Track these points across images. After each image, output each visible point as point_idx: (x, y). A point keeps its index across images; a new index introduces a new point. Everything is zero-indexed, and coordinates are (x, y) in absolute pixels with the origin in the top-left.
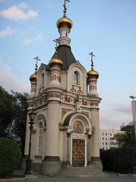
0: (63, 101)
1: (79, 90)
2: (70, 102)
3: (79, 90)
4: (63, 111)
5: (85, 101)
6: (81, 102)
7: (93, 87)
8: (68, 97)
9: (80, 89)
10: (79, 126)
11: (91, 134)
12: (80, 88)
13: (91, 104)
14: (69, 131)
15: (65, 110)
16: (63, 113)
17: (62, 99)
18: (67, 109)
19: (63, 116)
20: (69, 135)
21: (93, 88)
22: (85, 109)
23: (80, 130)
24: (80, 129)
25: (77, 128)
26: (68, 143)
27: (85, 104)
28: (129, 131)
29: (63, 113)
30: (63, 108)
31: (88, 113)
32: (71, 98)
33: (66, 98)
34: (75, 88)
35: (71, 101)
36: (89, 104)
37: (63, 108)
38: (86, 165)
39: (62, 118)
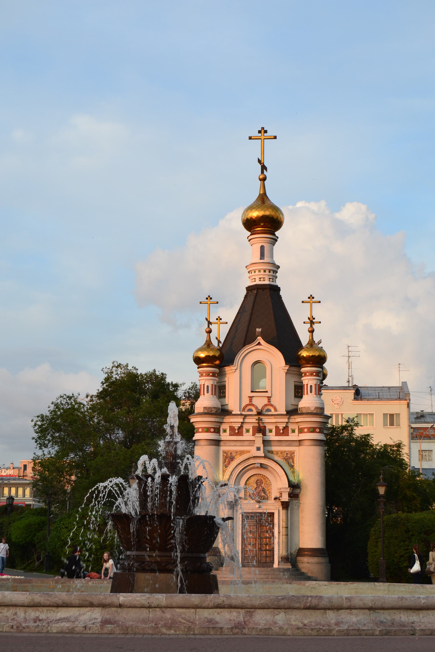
0: (225, 436)
1: (266, 402)
2: (242, 435)
3: (266, 402)
4: (225, 458)
5: (281, 426)
6: (274, 431)
7: (307, 389)
9: (269, 401)
10: (263, 485)
11: (287, 500)
12: (269, 398)
13: (301, 431)
15: (231, 453)
16: (227, 460)
17: (225, 431)
19: (226, 467)
21: (316, 387)
22: (284, 443)
23: (264, 493)
24: (264, 491)
27: (285, 431)
29: (227, 460)
30: (224, 452)
33: (232, 429)
34: (255, 401)
35: (248, 431)
36: (297, 431)
38: (276, 565)
39: (224, 472)
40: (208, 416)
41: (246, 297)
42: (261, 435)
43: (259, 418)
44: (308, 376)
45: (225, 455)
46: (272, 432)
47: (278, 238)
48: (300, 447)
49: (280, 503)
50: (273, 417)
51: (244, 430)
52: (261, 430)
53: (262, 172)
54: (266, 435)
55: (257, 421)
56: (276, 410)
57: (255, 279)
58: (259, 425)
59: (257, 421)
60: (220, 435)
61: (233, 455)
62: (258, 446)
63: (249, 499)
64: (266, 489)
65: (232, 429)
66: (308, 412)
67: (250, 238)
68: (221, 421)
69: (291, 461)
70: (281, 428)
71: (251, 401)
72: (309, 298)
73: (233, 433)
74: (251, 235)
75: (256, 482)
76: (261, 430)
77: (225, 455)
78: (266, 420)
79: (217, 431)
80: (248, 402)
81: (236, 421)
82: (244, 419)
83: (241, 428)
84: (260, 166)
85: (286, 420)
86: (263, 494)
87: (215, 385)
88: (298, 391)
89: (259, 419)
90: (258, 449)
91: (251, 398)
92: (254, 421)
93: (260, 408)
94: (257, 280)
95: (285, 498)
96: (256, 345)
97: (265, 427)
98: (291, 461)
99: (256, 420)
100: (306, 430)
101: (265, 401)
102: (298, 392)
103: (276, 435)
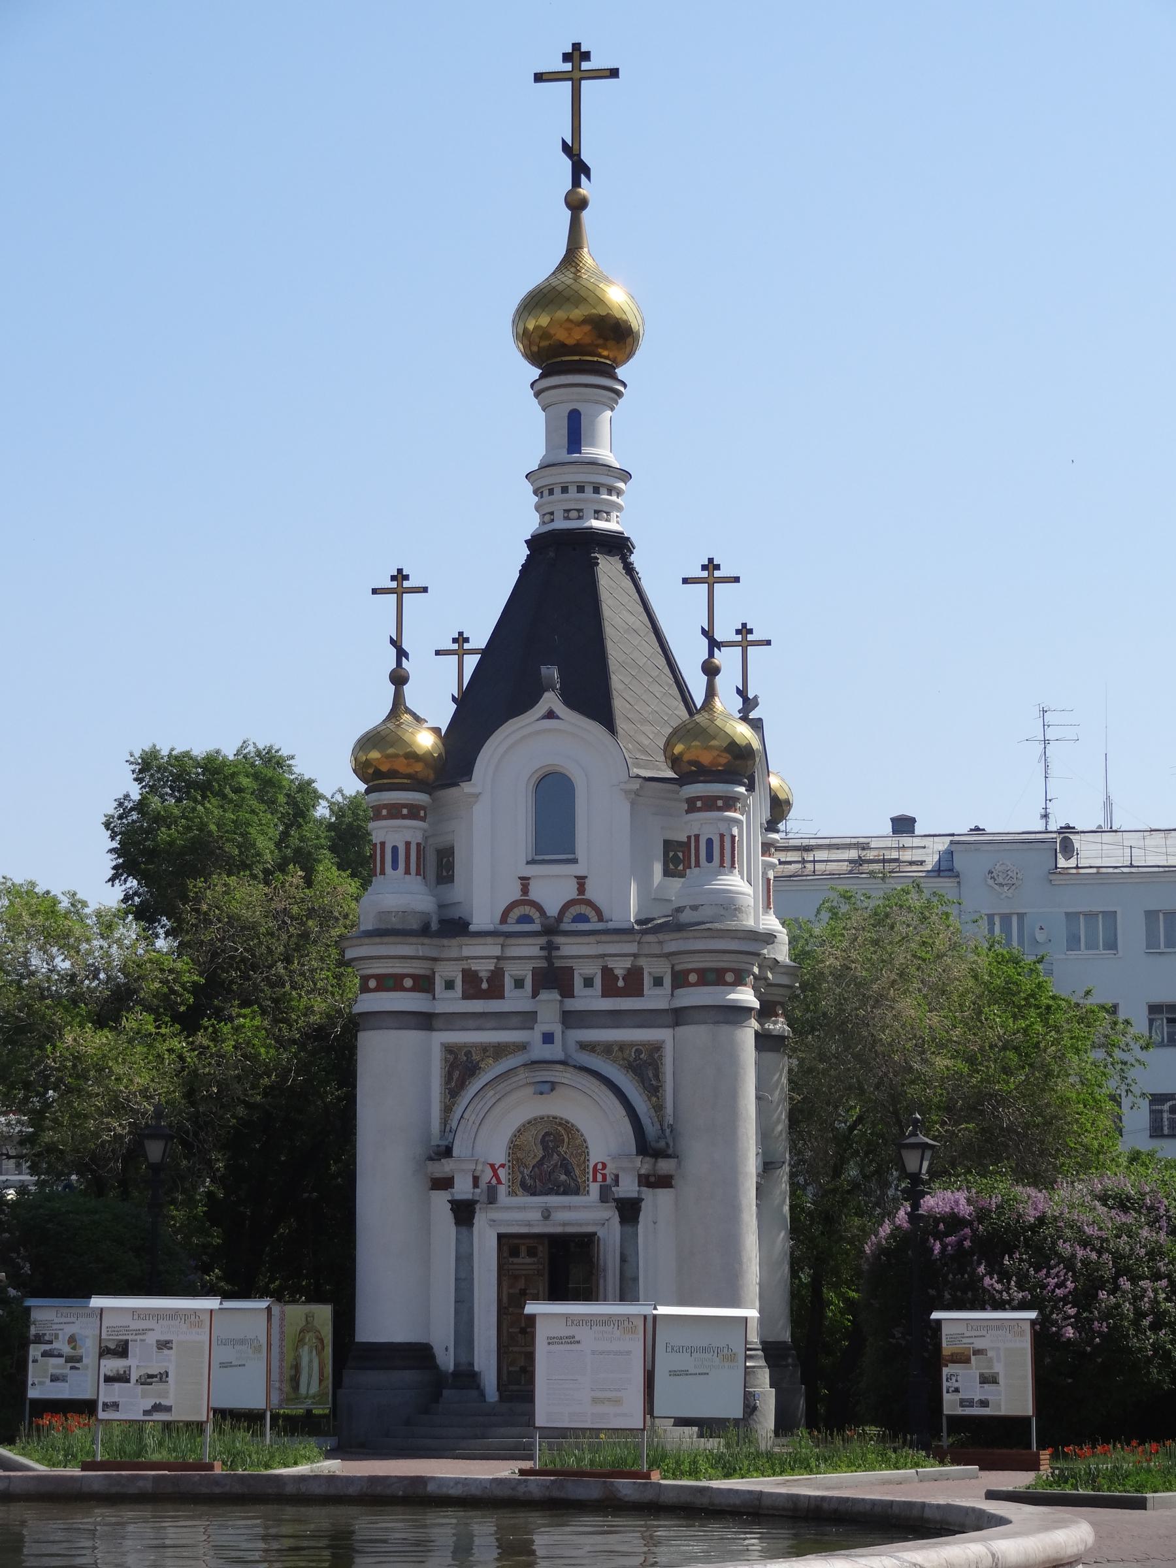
0: (450, 1002)
2: (502, 997)
3: (571, 892)
5: (620, 967)
6: (598, 982)
8: (484, 968)
9: (581, 889)
10: (562, 1150)
12: (581, 881)
13: (680, 980)
14: (463, 1189)
16: (456, 1074)
17: (449, 985)
18: (484, 1048)
20: (464, 1213)
23: (568, 1173)
24: (566, 1168)
25: (540, 1163)
26: (464, 1260)
27: (633, 984)
28: (918, 1153)
29: (456, 1074)
30: (449, 1049)
31: (656, 1048)
32: (512, 971)
33: (470, 978)
36: (667, 981)
37: (449, 1049)
40: (377, 940)
41: (525, 570)
42: (555, 995)
43: (550, 943)
44: (699, 810)
45: (451, 1057)
46: (585, 986)
47: (625, 385)
48: (677, 1029)
49: (614, 1204)
50: (591, 939)
51: (508, 983)
52: (554, 977)
53: (576, 183)
54: (573, 997)
55: (543, 953)
56: (601, 919)
57: (552, 513)
58: (551, 964)
59: (543, 953)
60: (434, 998)
61: (476, 1057)
62: (546, 1028)
63: (520, 1191)
64: (574, 1161)
65: (470, 978)
66: (383, 926)
67: (539, 386)
68: (434, 954)
69: (651, 1075)
70: (619, 972)
71: (525, 890)
72: (704, 568)
73: (472, 991)
74: (542, 376)
75: (543, 1142)
76: (554, 977)
77: (451, 1057)
78: (569, 948)
79: (424, 984)
80: (516, 895)
81: (480, 955)
82: (502, 946)
83: (497, 976)
84: (567, 164)
85: (632, 948)
86: (563, 1177)
87: (418, 845)
88: (676, 856)
89: (550, 947)
90: (548, 1038)
91: (525, 882)
92: (535, 951)
93: (552, 910)
94: (559, 514)
95: (628, 1188)
96: (544, 717)
97: (571, 970)
98: (651, 1075)
99: (541, 949)
100: (693, 978)
101: (570, 891)
102: (676, 860)
103: (603, 996)
